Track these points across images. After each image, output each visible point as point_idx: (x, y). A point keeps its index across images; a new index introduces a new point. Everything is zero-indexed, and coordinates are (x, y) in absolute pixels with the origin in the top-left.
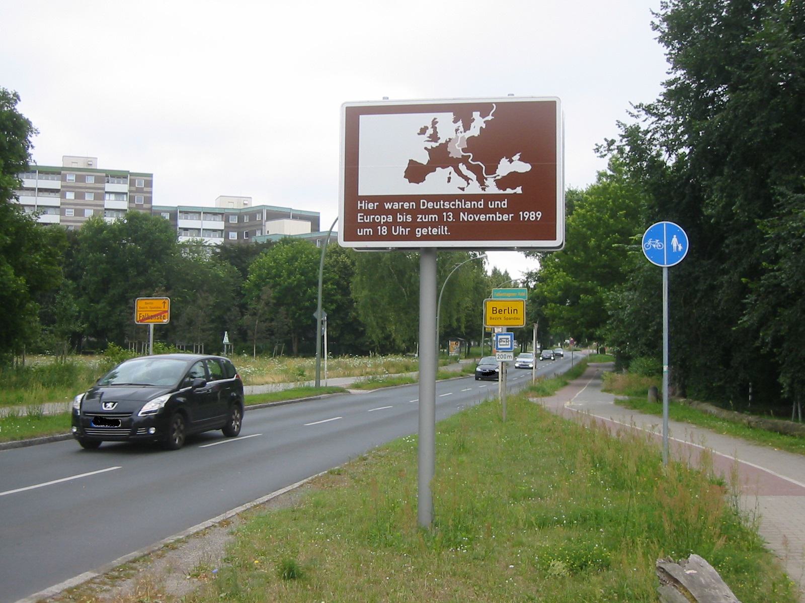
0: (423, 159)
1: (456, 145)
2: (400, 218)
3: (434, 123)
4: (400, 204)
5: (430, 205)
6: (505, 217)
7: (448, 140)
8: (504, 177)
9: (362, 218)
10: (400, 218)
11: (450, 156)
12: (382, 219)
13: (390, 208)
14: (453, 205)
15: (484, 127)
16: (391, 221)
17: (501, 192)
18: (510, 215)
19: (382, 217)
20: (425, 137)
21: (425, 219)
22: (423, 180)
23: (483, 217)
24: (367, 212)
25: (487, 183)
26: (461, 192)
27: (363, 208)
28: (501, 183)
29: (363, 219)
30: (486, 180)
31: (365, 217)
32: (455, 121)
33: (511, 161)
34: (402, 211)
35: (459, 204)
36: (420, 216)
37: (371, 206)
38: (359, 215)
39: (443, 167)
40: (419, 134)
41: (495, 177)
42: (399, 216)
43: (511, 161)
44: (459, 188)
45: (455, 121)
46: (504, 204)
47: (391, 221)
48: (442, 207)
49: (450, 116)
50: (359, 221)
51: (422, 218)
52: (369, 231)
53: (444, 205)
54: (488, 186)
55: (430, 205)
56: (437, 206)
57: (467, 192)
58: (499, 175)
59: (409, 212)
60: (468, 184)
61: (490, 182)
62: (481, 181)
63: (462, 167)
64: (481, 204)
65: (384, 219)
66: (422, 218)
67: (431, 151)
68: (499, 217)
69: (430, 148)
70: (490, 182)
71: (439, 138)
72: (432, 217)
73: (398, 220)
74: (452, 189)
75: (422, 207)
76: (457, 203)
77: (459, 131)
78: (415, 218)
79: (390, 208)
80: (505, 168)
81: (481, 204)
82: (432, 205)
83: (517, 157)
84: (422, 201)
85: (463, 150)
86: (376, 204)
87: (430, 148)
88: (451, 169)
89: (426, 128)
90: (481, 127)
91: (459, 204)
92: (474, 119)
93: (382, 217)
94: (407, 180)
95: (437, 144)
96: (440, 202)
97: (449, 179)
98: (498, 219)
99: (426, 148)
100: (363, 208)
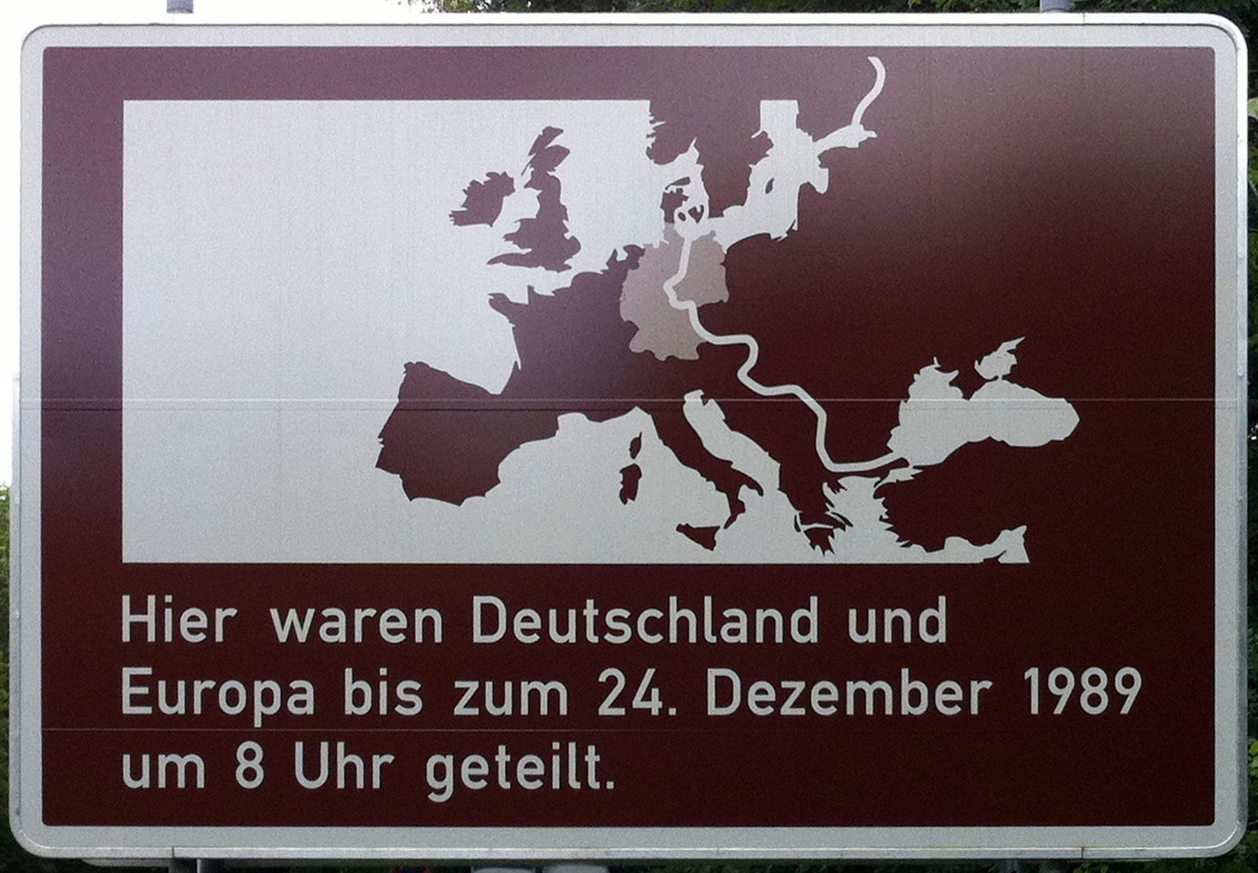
0: (486, 359)
1: (668, 286)
2: (358, 695)
3: (547, 153)
4: (360, 615)
5: (525, 625)
6: (947, 697)
7: (622, 256)
8: (927, 470)
9: (144, 690)
10: (358, 698)
11: (637, 345)
12: (262, 699)
13: (302, 636)
14: (652, 625)
15: (822, 186)
16: (309, 709)
17: (917, 555)
18: (976, 687)
19: (259, 687)
20: (490, 238)
21: (499, 701)
22: (483, 481)
23: (823, 696)
24: (175, 661)
25: (839, 503)
26: (695, 554)
27: (151, 637)
28: (920, 506)
29: (151, 699)
30: (836, 488)
31: (162, 685)
32: (662, 152)
33: (969, 384)
34: (369, 656)
35: (683, 622)
36: (473, 686)
37: (192, 624)
38: (127, 672)
39: (599, 413)
40: (460, 219)
41: (882, 472)
42: (350, 687)
43: (969, 384)
44: (685, 529)
45: (662, 152)
46: (934, 624)
47: (309, 709)
48: (592, 638)
49: (632, 119)
50: (127, 709)
51: (478, 700)
52: (185, 766)
53: (601, 627)
54: (844, 523)
55: (525, 625)
56: (563, 629)
57: (735, 548)
58: (902, 463)
59: (405, 660)
60: (737, 508)
61: (856, 499)
62: (807, 492)
63: (703, 415)
64: (804, 624)
65: (267, 698)
66: (478, 700)
67: (528, 319)
68: (912, 697)
69: (523, 299)
70: (856, 499)
71: (574, 246)
72: (534, 695)
73: (350, 708)
74: (647, 535)
75: (478, 638)
76: (674, 615)
77: (685, 208)
78: (439, 699)
79: (302, 636)
80: (935, 419)
81: (804, 624)
82: (537, 624)
83: (999, 361)
84: (478, 601)
85: (711, 316)
86: (220, 614)
87: (523, 299)
88: (639, 421)
89: (500, 185)
90: (806, 191)
91: (683, 622)
92: (763, 146)
93: (259, 687)
94: (397, 480)
95: (564, 280)
96: (581, 608)
97: (631, 481)
98: (906, 709)
99: (499, 302)
100: (151, 637)
